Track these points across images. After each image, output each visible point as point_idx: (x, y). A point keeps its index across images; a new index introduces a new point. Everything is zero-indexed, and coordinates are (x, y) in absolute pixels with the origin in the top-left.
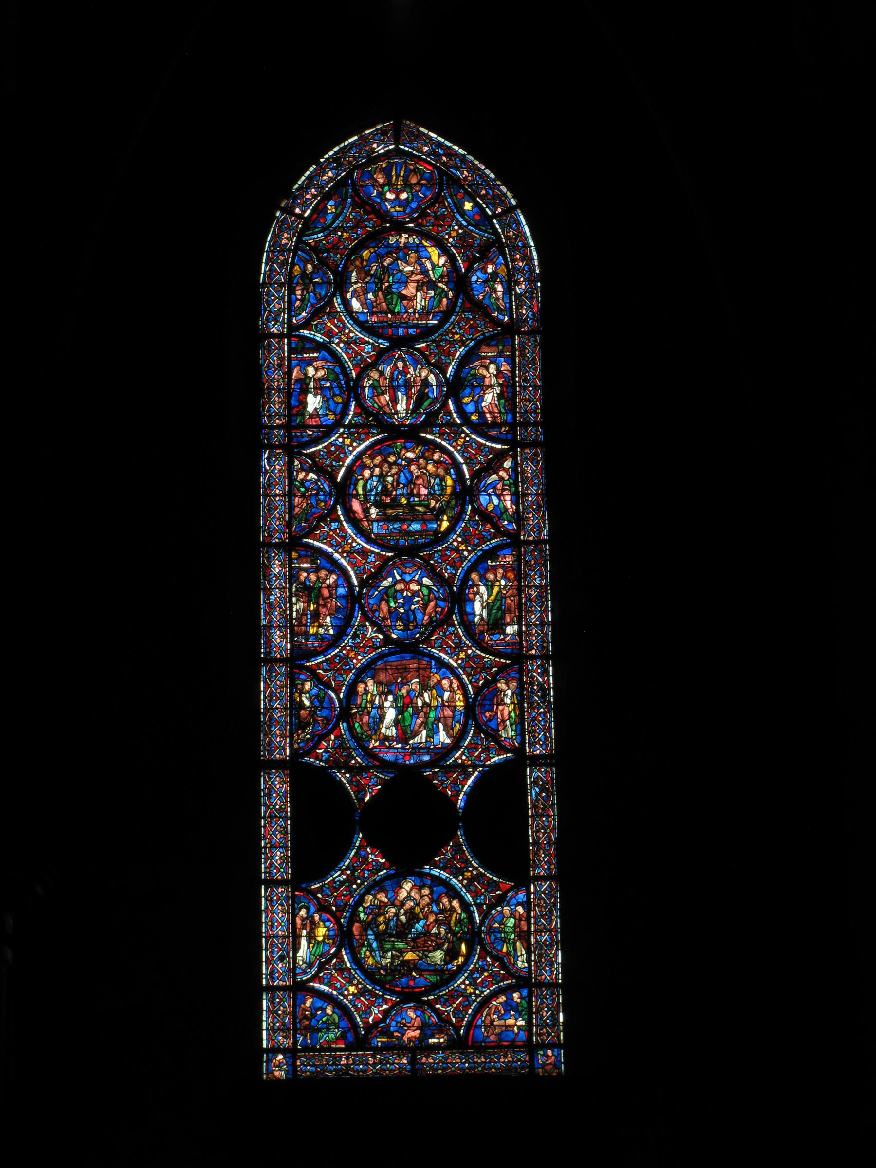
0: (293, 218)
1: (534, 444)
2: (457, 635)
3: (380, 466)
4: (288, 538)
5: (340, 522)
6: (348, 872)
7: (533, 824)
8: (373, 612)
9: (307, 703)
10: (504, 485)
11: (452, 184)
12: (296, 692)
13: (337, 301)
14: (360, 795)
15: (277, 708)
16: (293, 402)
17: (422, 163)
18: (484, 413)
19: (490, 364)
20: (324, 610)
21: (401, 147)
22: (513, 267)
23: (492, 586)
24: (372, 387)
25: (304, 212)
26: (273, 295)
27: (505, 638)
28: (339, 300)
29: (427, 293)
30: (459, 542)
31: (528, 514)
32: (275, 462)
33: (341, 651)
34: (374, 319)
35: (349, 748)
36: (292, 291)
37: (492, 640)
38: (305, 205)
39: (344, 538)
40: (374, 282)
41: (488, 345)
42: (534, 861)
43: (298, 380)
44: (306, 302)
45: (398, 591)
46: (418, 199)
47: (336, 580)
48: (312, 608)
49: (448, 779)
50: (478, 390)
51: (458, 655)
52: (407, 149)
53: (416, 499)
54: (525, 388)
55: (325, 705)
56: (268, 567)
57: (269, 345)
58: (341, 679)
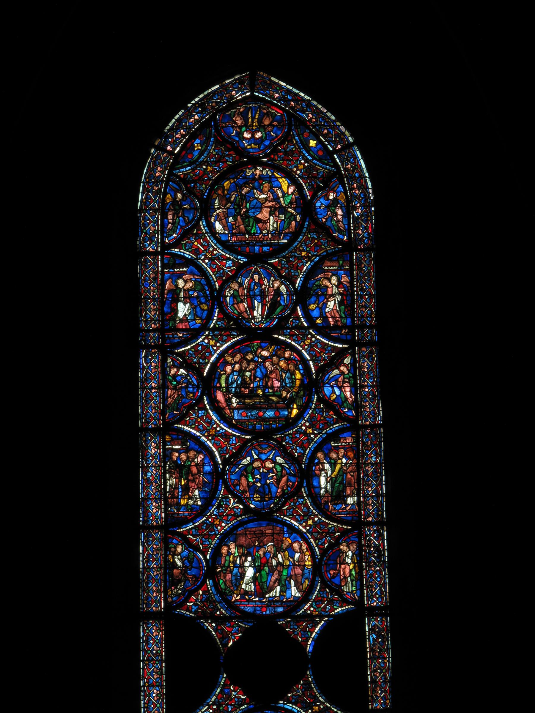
1: (370, 344)
2: (306, 505)
3: (240, 362)
4: (163, 424)
5: (206, 410)
6: (215, 707)
7: (371, 665)
8: (235, 486)
9: (179, 563)
10: (344, 378)
12: (170, 554)
13: (203, 224)
14: (224, 642)
15: (153, 568)
16: (166, 309)
18: (327, 317)
19: (332, 276)
20: (193, 484)
21: (255, 94)
23: (335, 464)
24: (233, 296)
25: (175, 149)
26: (149, 219)
27: (346, 508)
28: (204, 223)
30: (306, 427)
31: (365, 402)
32: (151, 359)
33: (207, 519)
34: (234, 239)
35: (215, 601)
36: (164, 216)
37: (335, 509)
38: (175, 143)
39: (209, 423)
40: (234, 208)
41: (330, 260)
42: (372, 697)
43: (170, 291)
44: (176, 225)
45: (256, 468)
46: (271, 138)
47: (203, 459)
48: (183, 483)
49: (298, 627)
50: (322, 299)
51: (306, 522)
52: (261, 96)
53: (270, 391)
54: (362, 296)
55: (194, 565)
56: (145, 449)
57: (146, 261)
58: (208, 543)
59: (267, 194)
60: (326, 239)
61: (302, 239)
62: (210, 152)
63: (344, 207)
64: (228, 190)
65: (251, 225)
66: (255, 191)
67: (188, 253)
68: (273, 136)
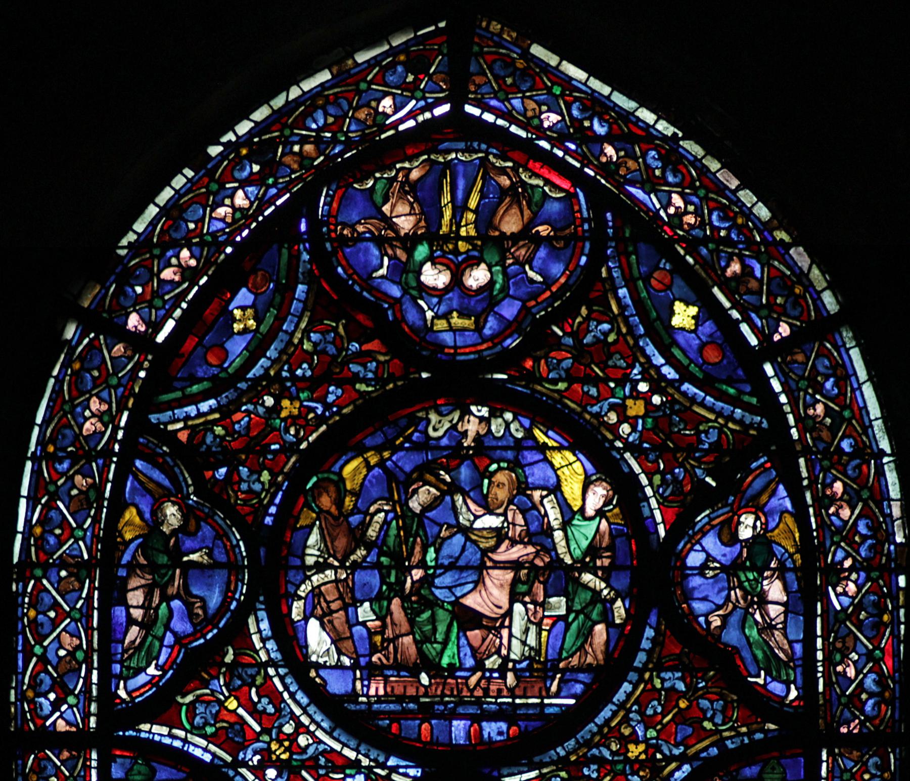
0: (119, 349)
11: (634, 239)
13: (259, 626)
17: (536, 166)
21: (469, 109)
22: (821, 524)
25: (158, 326)
26: (56, 606)
28: (265, 625)
29: (543, 605)
34: (377, 688)
36: (114, 593)
38: (156, 303)
40: (377, 565)
44: (159, 630)
46: (524, 290)
52: (489, 117)
59: (505, 514)
60: (722, 697)
61: (629, 695)
62: (290, 343)
63: (795, 570)
64: (356, 494)
65: (440, 637)
66: (459, 499)
67: (203, 743)
68: (532, 281)
